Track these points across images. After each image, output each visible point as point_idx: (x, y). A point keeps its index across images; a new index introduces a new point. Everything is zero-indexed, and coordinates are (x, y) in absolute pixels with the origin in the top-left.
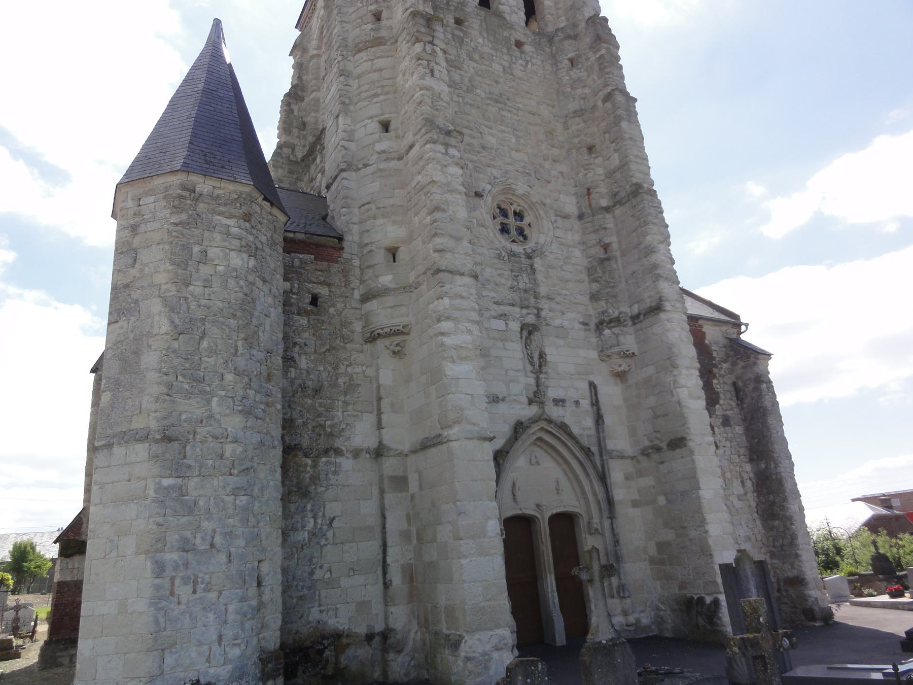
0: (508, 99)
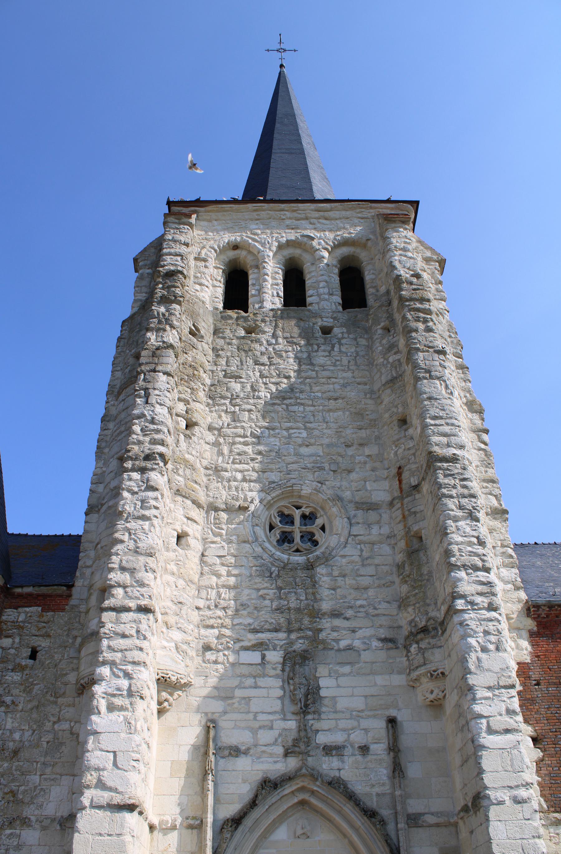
0: (301, 392)
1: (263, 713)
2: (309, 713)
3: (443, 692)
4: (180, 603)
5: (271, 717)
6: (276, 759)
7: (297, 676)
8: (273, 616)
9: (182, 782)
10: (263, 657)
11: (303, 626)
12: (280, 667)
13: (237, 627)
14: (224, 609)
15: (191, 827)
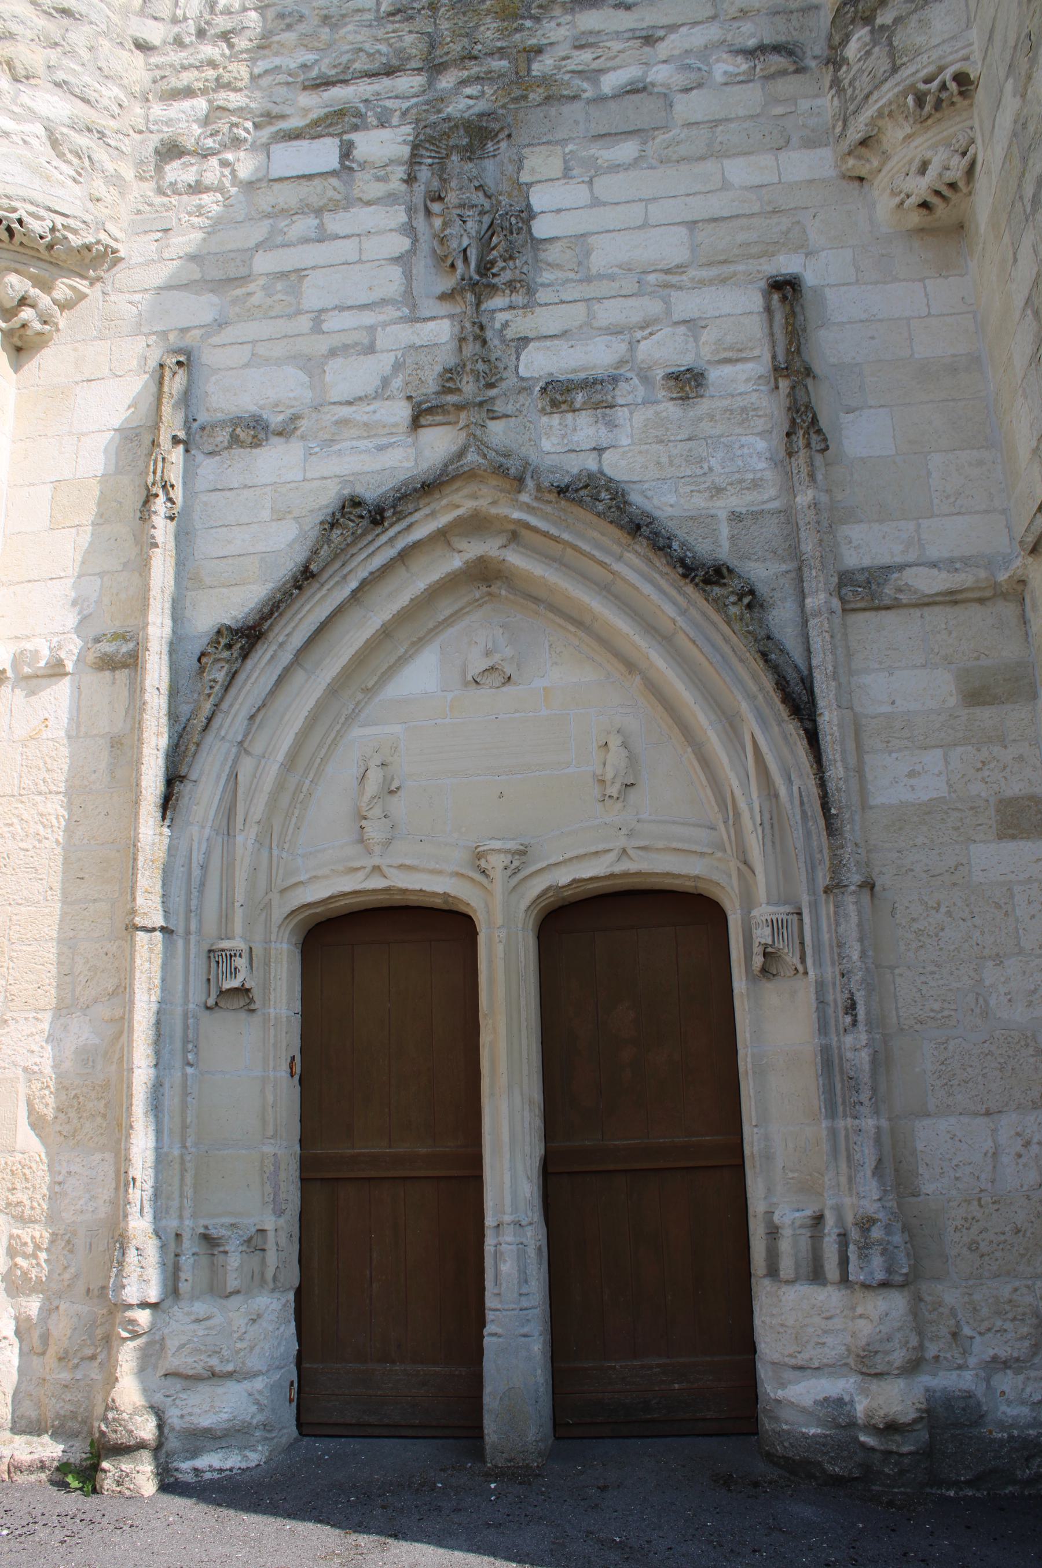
1: (341, 308)
2: (493, 288)
3: (964, 154)
4: (65, 12)
5: (368, 318)
6: (384, 441)
7: (453, 184)
8: (380, 33)
9: (85, 538)
10: (346, 151)
11: (479, 47)
12: (400, 172)
13: (265, 82)
14: (225, 36)
15: (108, 664)
